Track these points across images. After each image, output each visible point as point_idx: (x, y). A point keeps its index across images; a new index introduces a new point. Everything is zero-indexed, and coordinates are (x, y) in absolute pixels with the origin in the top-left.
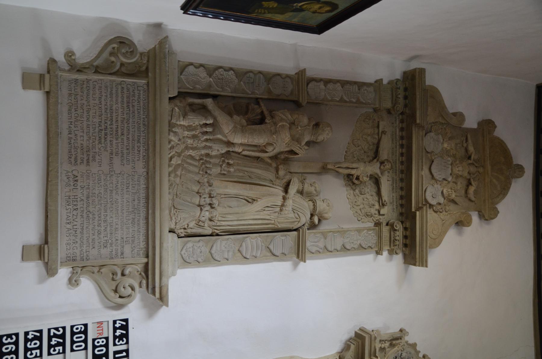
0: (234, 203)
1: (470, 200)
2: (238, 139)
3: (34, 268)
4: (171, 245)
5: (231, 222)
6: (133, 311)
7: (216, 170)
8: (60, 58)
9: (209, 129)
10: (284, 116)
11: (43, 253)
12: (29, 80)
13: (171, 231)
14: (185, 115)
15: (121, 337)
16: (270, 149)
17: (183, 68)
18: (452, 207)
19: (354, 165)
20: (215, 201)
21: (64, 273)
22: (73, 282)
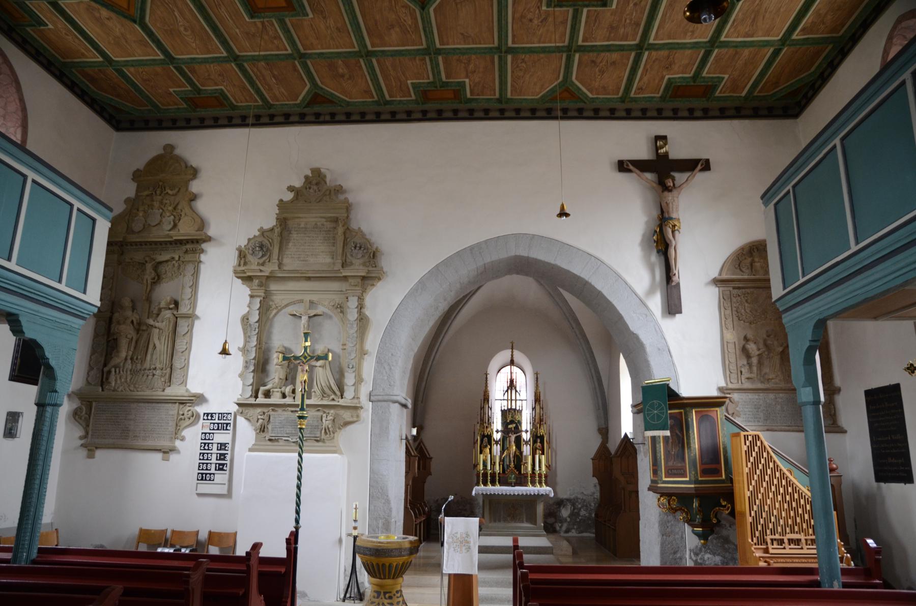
0: (154, 357)
2: (123, 354)
3: (173, 457)
4: (174, 391)
5: (165, 358)
7: (139, 366)
8: (82, 442)
10: (114, 328)
11: (167, 452)
12: (91, 455)
13: (164, 390)
14: (110, 383)
15: (212, 416)
16: (129, 336)
17: (88, 383)
18: (180, 207)
20: (153, 366)
21: (178, 443)
22: (183, 439)
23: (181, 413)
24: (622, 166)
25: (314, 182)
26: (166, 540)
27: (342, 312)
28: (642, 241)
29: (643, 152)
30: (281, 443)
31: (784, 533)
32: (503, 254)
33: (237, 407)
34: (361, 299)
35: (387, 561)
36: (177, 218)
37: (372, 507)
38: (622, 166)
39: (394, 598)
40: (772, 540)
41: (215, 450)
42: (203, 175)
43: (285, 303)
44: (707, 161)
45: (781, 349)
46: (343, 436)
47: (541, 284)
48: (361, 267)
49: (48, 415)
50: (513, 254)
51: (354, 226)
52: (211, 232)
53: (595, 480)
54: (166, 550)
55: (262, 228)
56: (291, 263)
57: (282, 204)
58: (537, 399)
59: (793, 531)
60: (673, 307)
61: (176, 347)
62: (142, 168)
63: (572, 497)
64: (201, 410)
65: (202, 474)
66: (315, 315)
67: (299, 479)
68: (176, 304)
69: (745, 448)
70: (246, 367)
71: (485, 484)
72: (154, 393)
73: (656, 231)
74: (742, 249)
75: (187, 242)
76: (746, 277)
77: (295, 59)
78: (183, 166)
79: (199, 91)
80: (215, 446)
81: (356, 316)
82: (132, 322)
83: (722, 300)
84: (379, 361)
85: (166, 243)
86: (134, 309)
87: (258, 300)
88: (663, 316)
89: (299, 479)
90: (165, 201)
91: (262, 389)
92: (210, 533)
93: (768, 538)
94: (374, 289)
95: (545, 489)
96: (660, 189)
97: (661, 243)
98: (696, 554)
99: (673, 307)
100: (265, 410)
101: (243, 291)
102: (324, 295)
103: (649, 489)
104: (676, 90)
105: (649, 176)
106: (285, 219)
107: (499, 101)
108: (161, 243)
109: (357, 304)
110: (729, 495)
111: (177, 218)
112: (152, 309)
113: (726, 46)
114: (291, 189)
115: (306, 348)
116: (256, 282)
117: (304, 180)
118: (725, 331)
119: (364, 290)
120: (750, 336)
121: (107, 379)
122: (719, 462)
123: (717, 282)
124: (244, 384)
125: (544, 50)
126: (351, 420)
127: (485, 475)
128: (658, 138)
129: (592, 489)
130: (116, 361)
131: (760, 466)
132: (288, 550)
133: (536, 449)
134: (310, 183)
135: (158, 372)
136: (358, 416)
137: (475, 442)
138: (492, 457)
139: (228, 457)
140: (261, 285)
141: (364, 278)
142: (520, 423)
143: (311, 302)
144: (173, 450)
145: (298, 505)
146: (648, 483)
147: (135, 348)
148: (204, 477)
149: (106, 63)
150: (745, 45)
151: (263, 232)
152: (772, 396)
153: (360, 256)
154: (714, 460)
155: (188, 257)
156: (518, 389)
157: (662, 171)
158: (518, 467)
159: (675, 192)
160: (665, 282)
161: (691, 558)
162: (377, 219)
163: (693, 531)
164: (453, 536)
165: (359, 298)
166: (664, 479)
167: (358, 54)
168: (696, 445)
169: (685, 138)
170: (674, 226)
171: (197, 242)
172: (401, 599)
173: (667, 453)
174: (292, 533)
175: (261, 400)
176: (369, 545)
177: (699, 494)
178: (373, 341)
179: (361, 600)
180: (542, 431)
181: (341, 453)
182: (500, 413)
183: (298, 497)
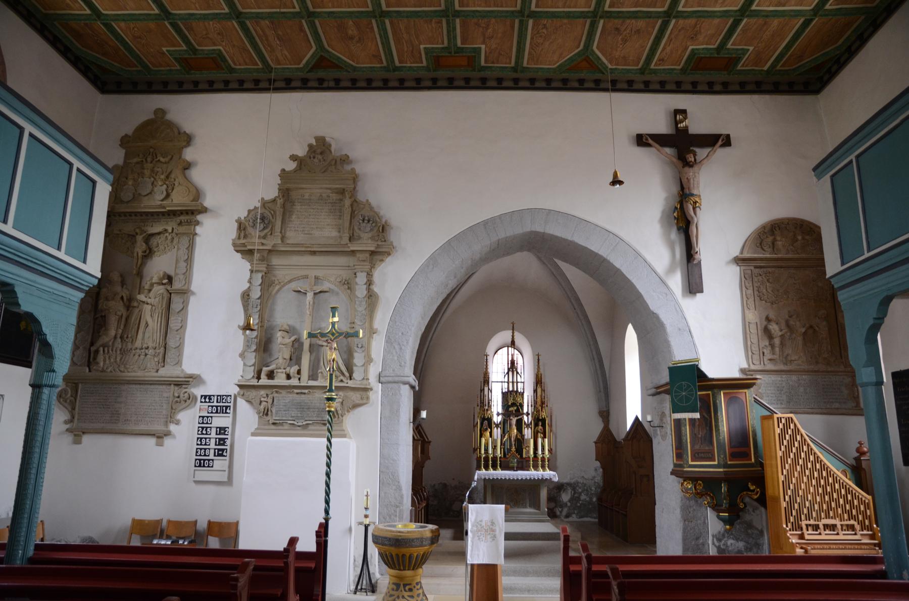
0: (147, 335)
1: (171, 159)
2: (112, 333)
3: (167, 441)
4: (167, 372)
5: (158, 337)
6: (198, 392)
7: (129, 346)
8: (68, 426)
9: (106, 349)
10: (102, 304)
11: (161, 437)
12: (77, 441)
13: (157, 371)
14: (98, 363)
15: (210, 399)
16: (119, 313)
17: (73, 363)
18: (173, 176)
19: (135, 255)
20: (145, 346)
21: (172, 427)
22: (178, 423)
23: (177, 395)
24: (641, 140)
25: (319, 151)
26: (162, 532)
27: (349, 288)
28: (662, 217)
29: (662, 127)
30: (286, 427)
31: (819, 518)
32: (516, 230)
33: (238, 389)
34: (369, 275)
35: (407, 551)
36: (170, 188)
37: (382, 494)
38: (641, 140)
39: (415, 590)
40: (807, 525)
41: (213, 435)
42: (198, 142)
43: (288, 278)
44: (728, 136)
45: (803, 330)
46: (350, 421)
47: (544, 263)
48: (370, 241)
49: (45, 397)
50: (528, 230)
51: (361, 197)
52: (208, 202)
53: (598, 464)
54: (163, 542)
55: (263, 199)
56: (294, 236)
57: (284, 174)
58: (538, 381)
59: (828, 516)
60: (693, 286)
61: (171, 324)
62: (130, 133)
63: (572, 481)
64: (198, 392)
65: (200, 460)
66: (320, 292)
67: (328, 465)
68: (170, 279)
69: (778, 431)
70: (247, 345)
71: (487, 468)
72: (147, 374)
73: (676, 208)
74: (764, 227)
75: (181, 213)
76: (768, 256)
77: (303, 18)
78: (176, 133)
79: (195, 51)
80: (214, 430)
81: (365, 292)
82: (122, 298)
83: (743, 279)
84: (388, 341)
85: (158, 213)
86: (123, 284)
87: (260, 275)
88: (684, 295)
89: (328, 465)
90: (156, 169)
91: (265, 369)
92: (210, 523)
93: (804, 523)
94: (383, 264)
95: (548, 474)
96: (680, 164)
97: (682, 220)
98: (719, 540)
99: (693, 286)
100: (269, 392)
101: (242, 266)
102: (330, 271)
103: (672, 473)
104: (698, 62)
105: (668, 150)
106: (288, 190)
107: (514, 69)
108: (152, 214)
109: (365, 280)
110: (760, 479)
111: (170, 188)
112: (143, 284)
113: (757, 16)
114: (293, 158)
115: (333, 324)
116: (257, 256)
117: (307, 149)
118: (747, 311)
119: (373, 267)
120: (772, 316)
121: (95, 359)
122: (748, 445)
123: (738, 261)
124: (245, 365)
125: (568, 15)
126: (361, 402)
127: (486, 459)
128: (677, 112)
129: (593, 473)
130: (105, 339)
131: (794, 450)
132: (318, 544)
133: (538, 432)
134: (314, 152)
135: (151, 352)
136: (368, 398)
137: (475, 426)
138: (493, 441)
139: (228, 442)
140: (262, 259)
141: (373, 253)
142: (522, 406)
143: (316, 278)
144: (168, 434)
145: (328, 494)
146: (671, 467)
147: (125, 326)
148: (202, 463)
149: (95, 17)
150: (775, 14)
151: (264, 204)
152: (794, 378)
153: (368, 229)
154: (743, 443)
155: (182, 229)
156: (519, 371)
157: (682, 146)
158: (519, 450)
159: (696, 168)
160: (685, 261)
161: (713, 544)
162: (388, 190)
163: (719, 517)
164: (478, 523)
165: (368, 274)
166: (691, 463)
167: (372, 14)
168: (724, 428)
169: (705, 112)
170: (695, 203)
171: (193, 212)
172: (421, 591)
173: (694, 436)
174: (321, 525)
175: (264, 381)
176: (389, 535)
177: (728, 479)
178: (382, 319)
179: (373, 591)
180: (543, 414)
181: (350, 438)
183: (328, 485)
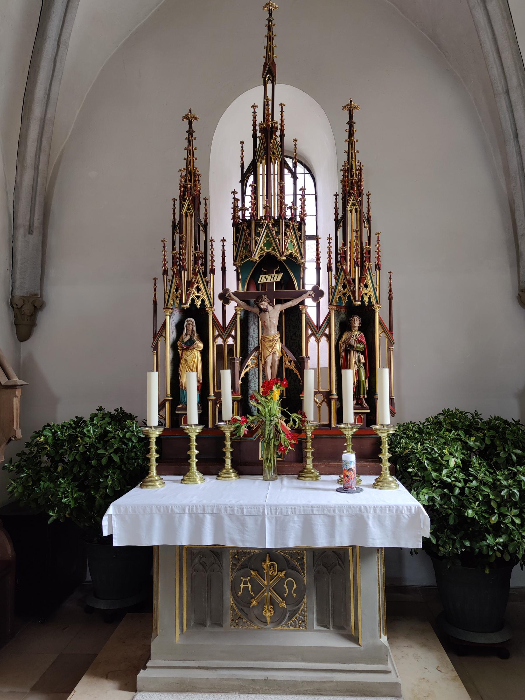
58: (351, 186)
133: (349, 348)
137: (159, 333)
142: (295, 265)
180: (367, 293)
182: (229, 234)
